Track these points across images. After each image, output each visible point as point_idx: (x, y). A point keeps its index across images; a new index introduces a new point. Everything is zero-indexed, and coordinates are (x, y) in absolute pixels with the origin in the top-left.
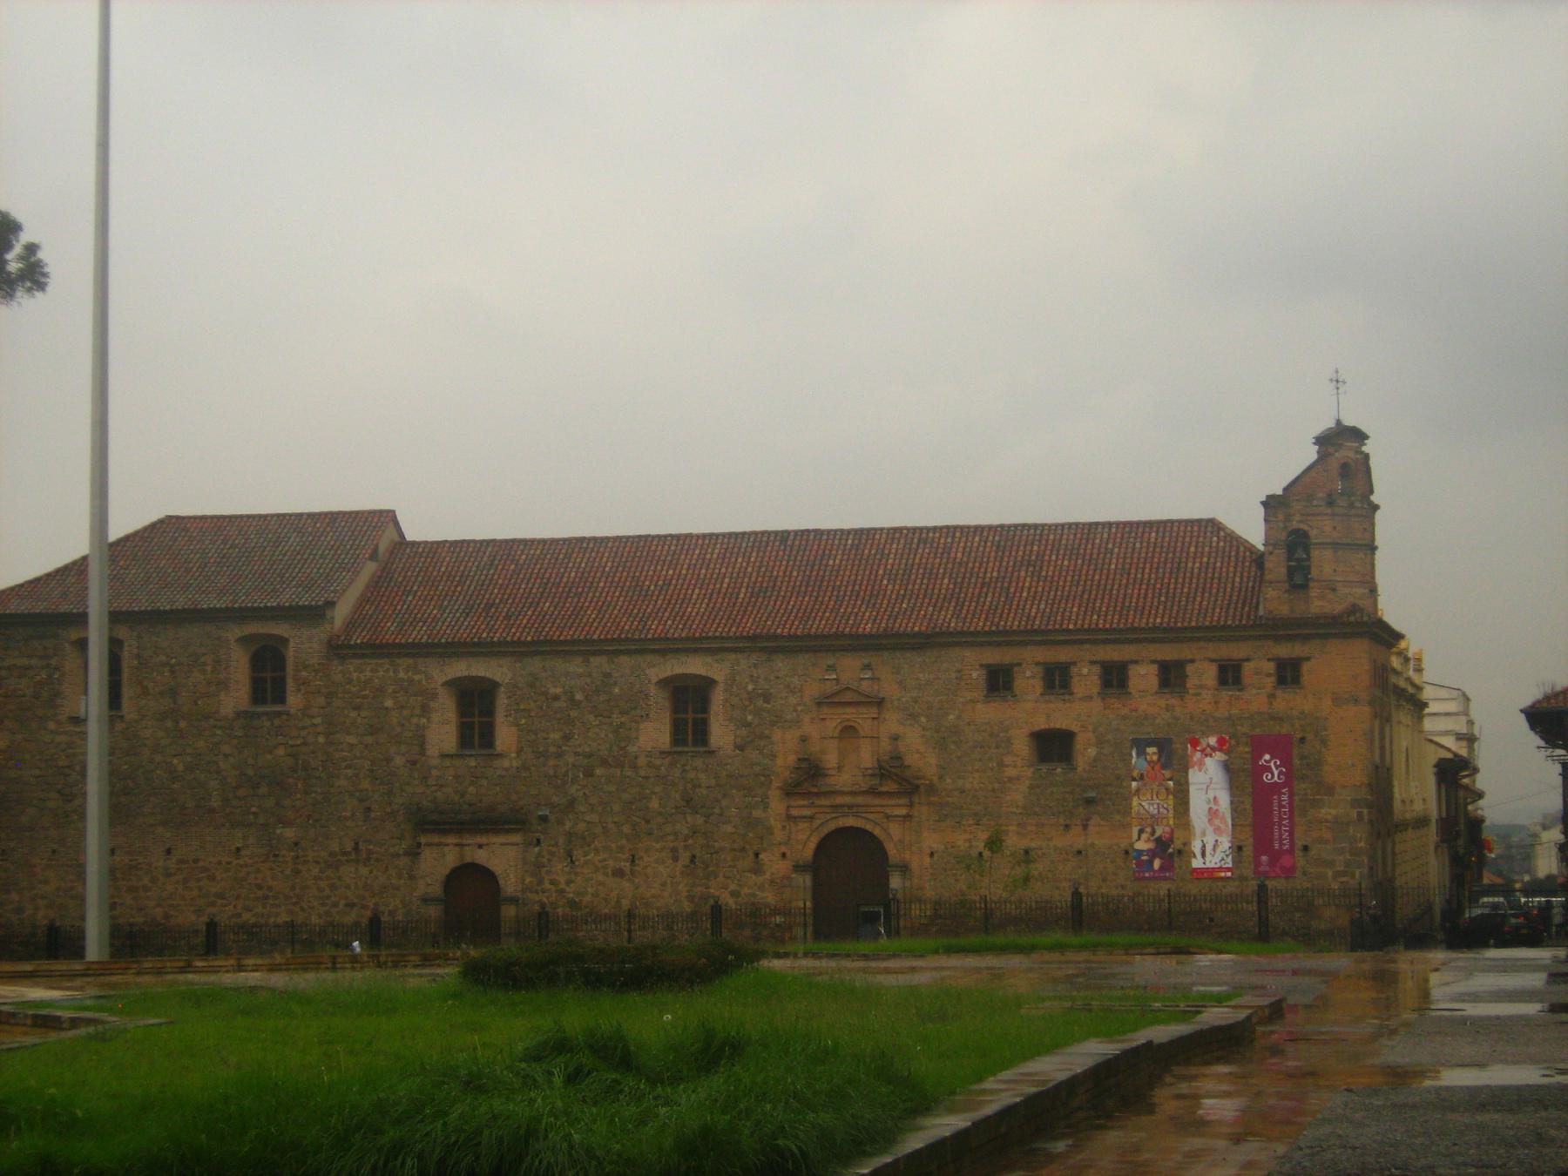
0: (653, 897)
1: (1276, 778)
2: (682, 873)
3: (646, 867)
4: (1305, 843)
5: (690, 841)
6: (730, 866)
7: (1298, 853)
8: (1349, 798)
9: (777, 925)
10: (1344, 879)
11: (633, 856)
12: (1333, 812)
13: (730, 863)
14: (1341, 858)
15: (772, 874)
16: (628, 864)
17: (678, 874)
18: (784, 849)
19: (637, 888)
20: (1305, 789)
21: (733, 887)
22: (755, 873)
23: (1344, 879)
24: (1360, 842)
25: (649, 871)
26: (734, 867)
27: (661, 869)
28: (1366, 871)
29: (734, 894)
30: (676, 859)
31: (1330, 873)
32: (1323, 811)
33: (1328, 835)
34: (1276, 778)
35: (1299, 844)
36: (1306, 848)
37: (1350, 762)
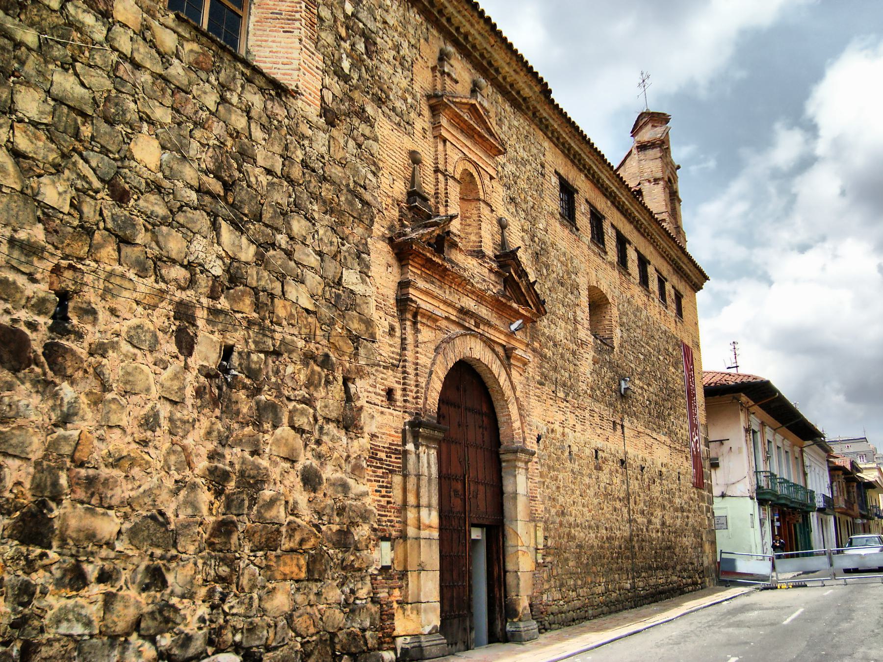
0: (117, 462)
2: (199, 392)
3: (99, 350)
5: (223, 303)
6: (304, 401)
9: (385, 569)
11: (64, 296)
13: (303, 392)
15: (373, 436)
16: (44, 321)
17: (189, 392)
18: (391, 379)
19: (65, 420)
21: (306, 459)
22: (346, 428)
25: (112, 364)
26: (308, 401)
27: (145, 364)
29: (311, 480)
30: (186, 344)
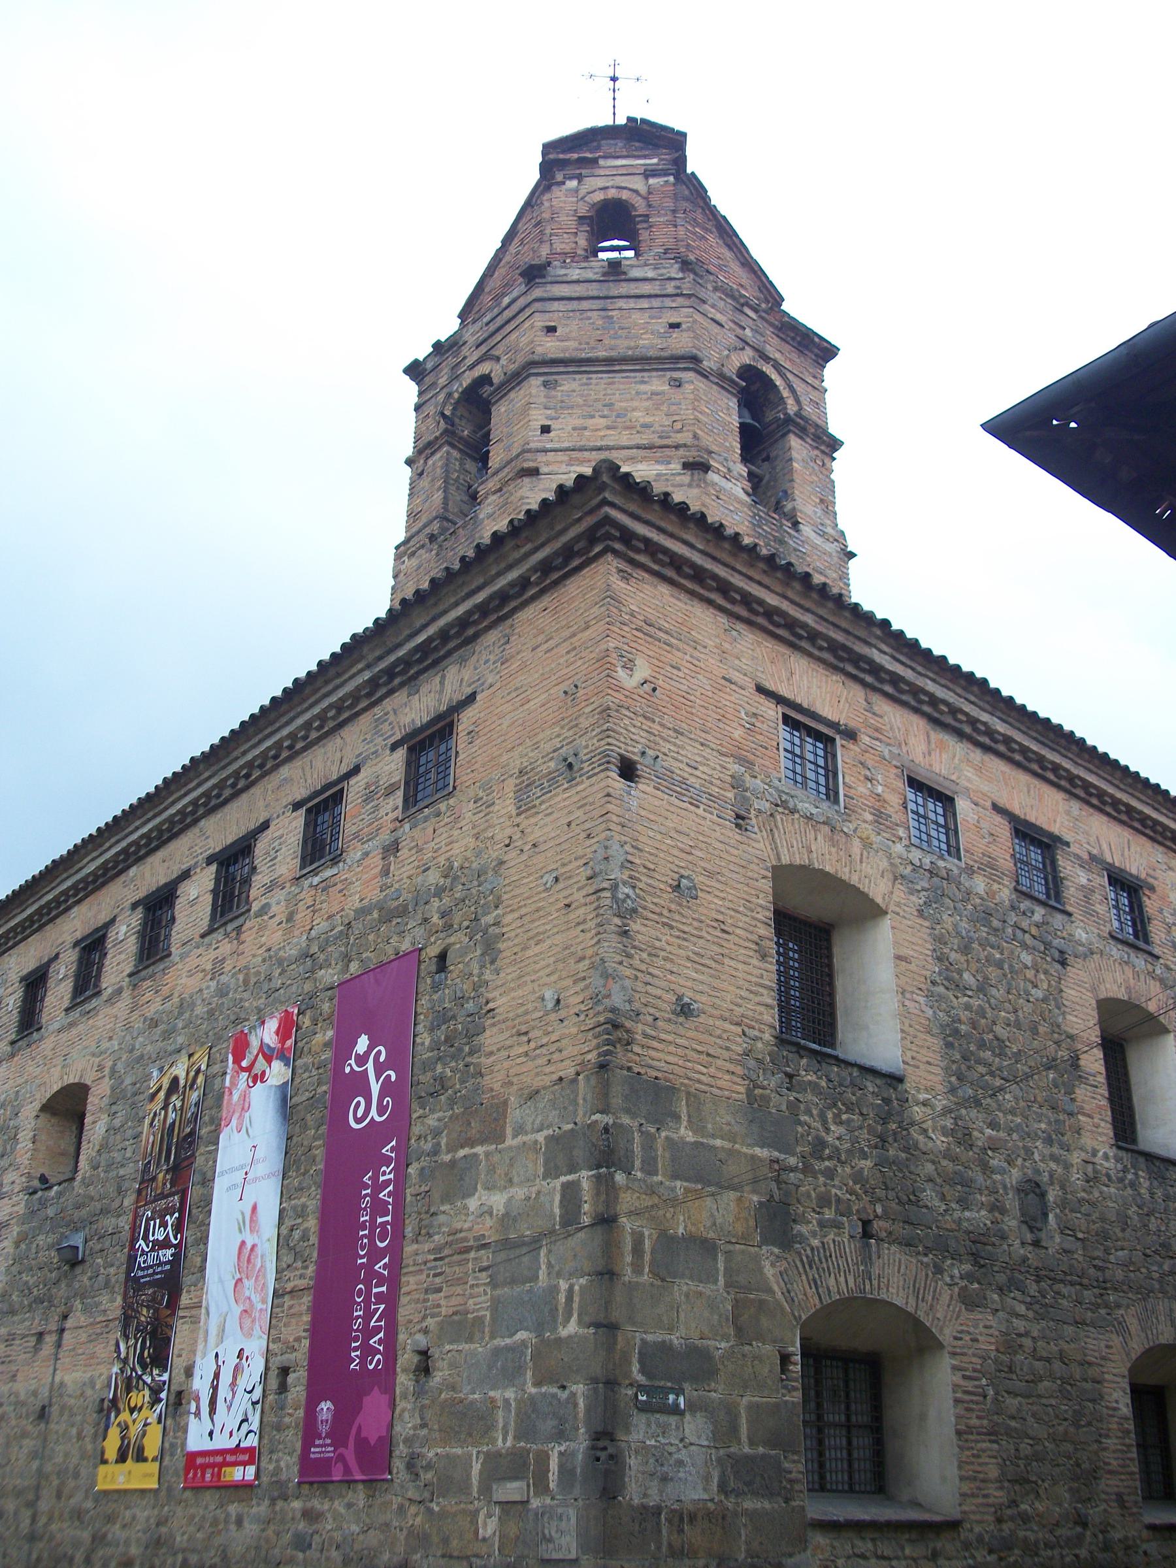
1: (373, 1112)
4: (422, 1341)
7: (404, 1381)
8: (541, 1137)
10: (512, 1490)
12: (498, 1201)
14: (510, 1394)
20: (437, 1133)
23: (512, 1490)
24: (567, 1320)
28: (580, 1444)
31: (476, 1468)
32: (473, 1204)
33: (480, 1303)
34: (373, 1112)
35: (409, 1341)
36: (424, 1366)
37: (549, 995)
